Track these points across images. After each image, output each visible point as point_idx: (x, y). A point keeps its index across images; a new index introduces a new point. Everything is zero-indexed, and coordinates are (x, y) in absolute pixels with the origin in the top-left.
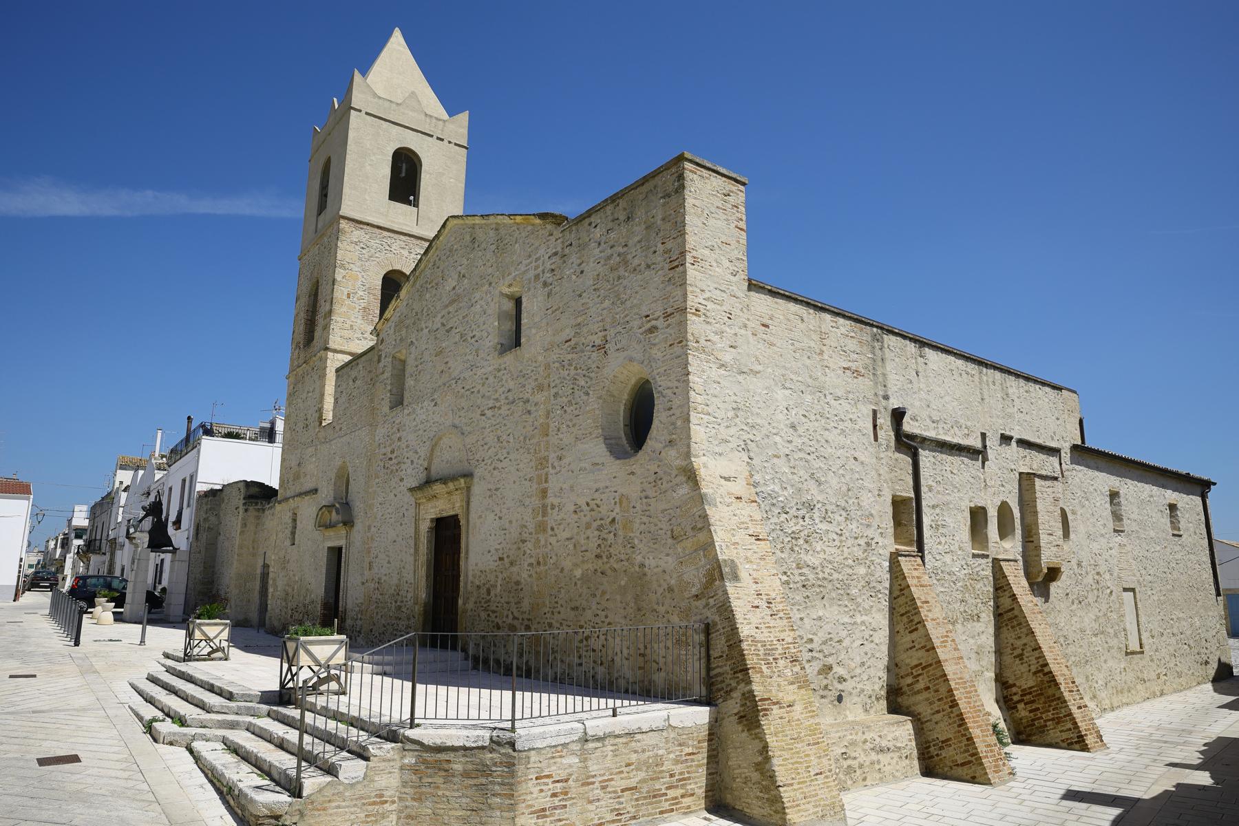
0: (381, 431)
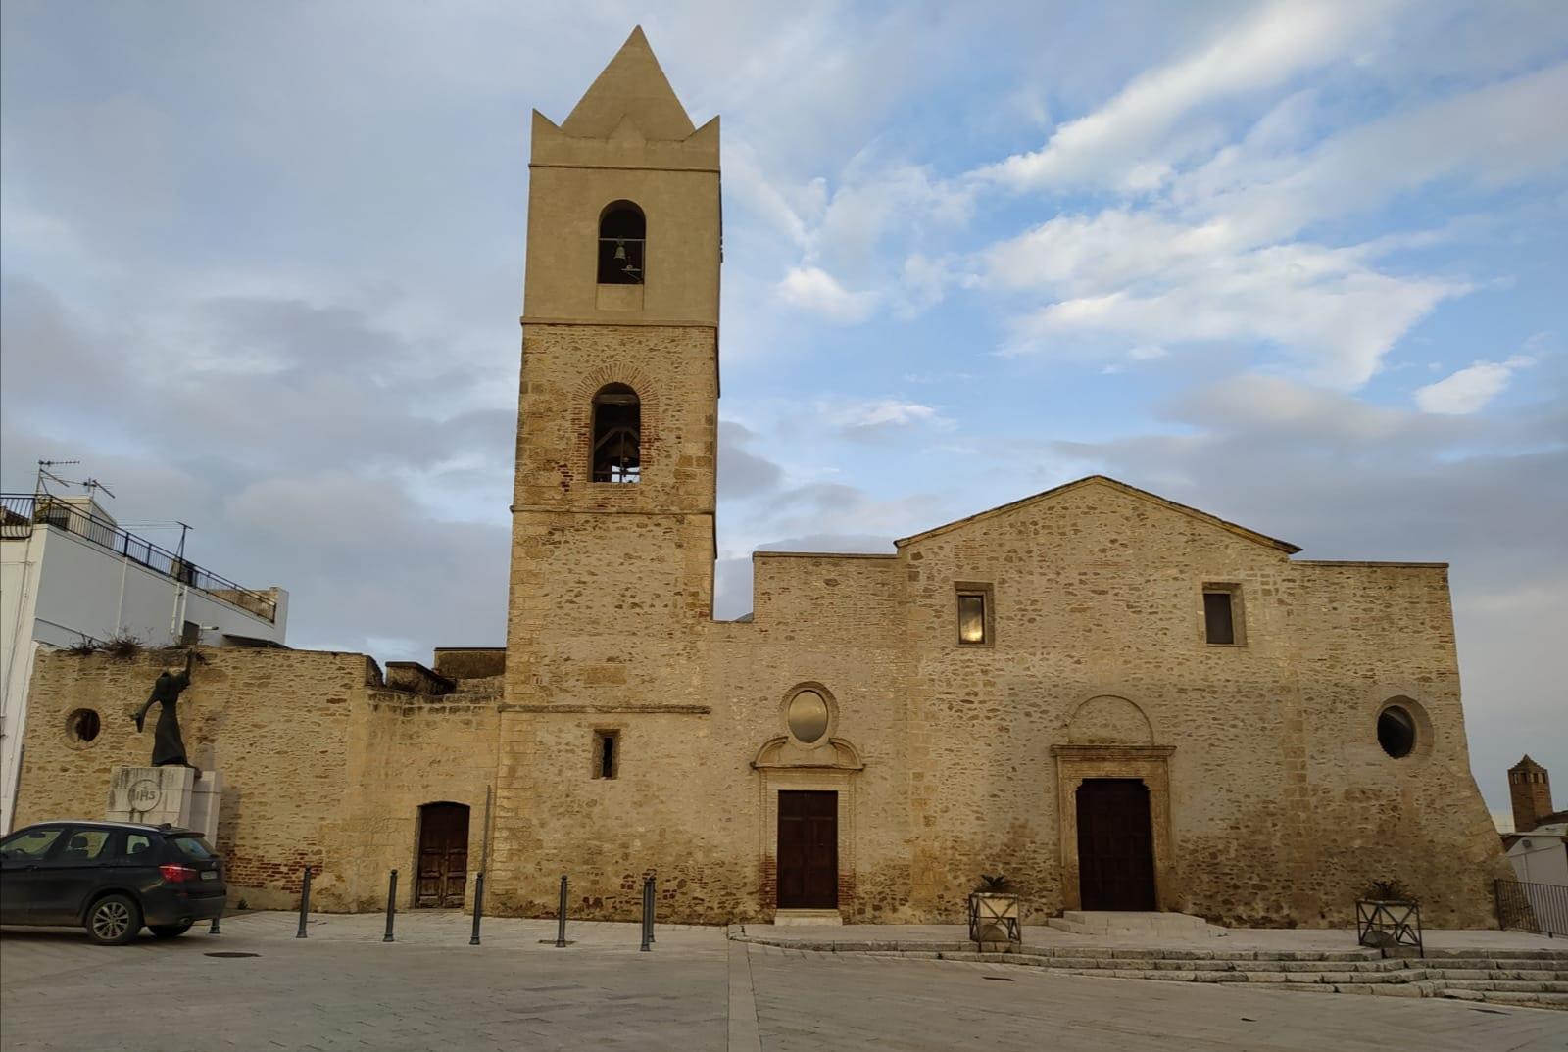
0: (928, 667)
